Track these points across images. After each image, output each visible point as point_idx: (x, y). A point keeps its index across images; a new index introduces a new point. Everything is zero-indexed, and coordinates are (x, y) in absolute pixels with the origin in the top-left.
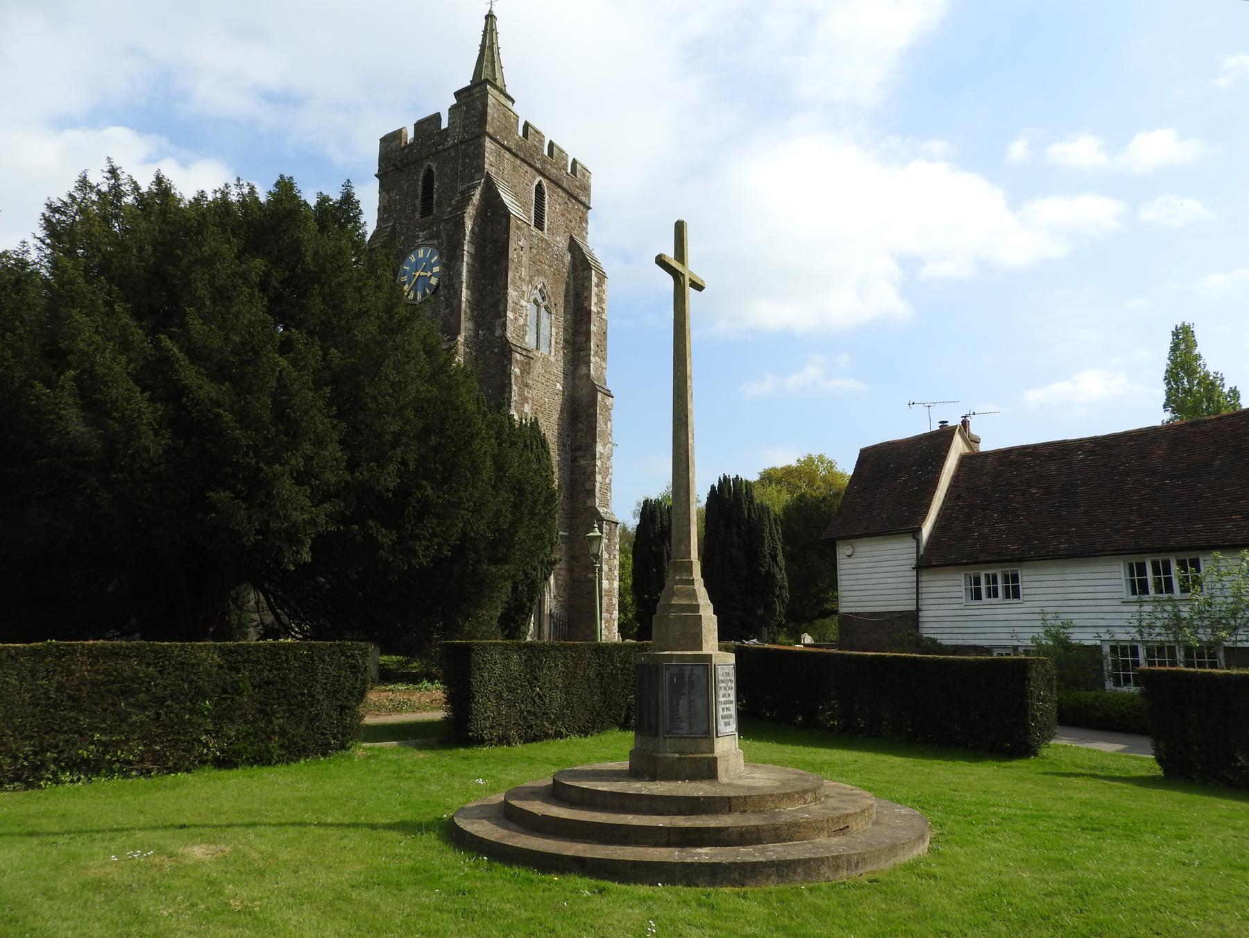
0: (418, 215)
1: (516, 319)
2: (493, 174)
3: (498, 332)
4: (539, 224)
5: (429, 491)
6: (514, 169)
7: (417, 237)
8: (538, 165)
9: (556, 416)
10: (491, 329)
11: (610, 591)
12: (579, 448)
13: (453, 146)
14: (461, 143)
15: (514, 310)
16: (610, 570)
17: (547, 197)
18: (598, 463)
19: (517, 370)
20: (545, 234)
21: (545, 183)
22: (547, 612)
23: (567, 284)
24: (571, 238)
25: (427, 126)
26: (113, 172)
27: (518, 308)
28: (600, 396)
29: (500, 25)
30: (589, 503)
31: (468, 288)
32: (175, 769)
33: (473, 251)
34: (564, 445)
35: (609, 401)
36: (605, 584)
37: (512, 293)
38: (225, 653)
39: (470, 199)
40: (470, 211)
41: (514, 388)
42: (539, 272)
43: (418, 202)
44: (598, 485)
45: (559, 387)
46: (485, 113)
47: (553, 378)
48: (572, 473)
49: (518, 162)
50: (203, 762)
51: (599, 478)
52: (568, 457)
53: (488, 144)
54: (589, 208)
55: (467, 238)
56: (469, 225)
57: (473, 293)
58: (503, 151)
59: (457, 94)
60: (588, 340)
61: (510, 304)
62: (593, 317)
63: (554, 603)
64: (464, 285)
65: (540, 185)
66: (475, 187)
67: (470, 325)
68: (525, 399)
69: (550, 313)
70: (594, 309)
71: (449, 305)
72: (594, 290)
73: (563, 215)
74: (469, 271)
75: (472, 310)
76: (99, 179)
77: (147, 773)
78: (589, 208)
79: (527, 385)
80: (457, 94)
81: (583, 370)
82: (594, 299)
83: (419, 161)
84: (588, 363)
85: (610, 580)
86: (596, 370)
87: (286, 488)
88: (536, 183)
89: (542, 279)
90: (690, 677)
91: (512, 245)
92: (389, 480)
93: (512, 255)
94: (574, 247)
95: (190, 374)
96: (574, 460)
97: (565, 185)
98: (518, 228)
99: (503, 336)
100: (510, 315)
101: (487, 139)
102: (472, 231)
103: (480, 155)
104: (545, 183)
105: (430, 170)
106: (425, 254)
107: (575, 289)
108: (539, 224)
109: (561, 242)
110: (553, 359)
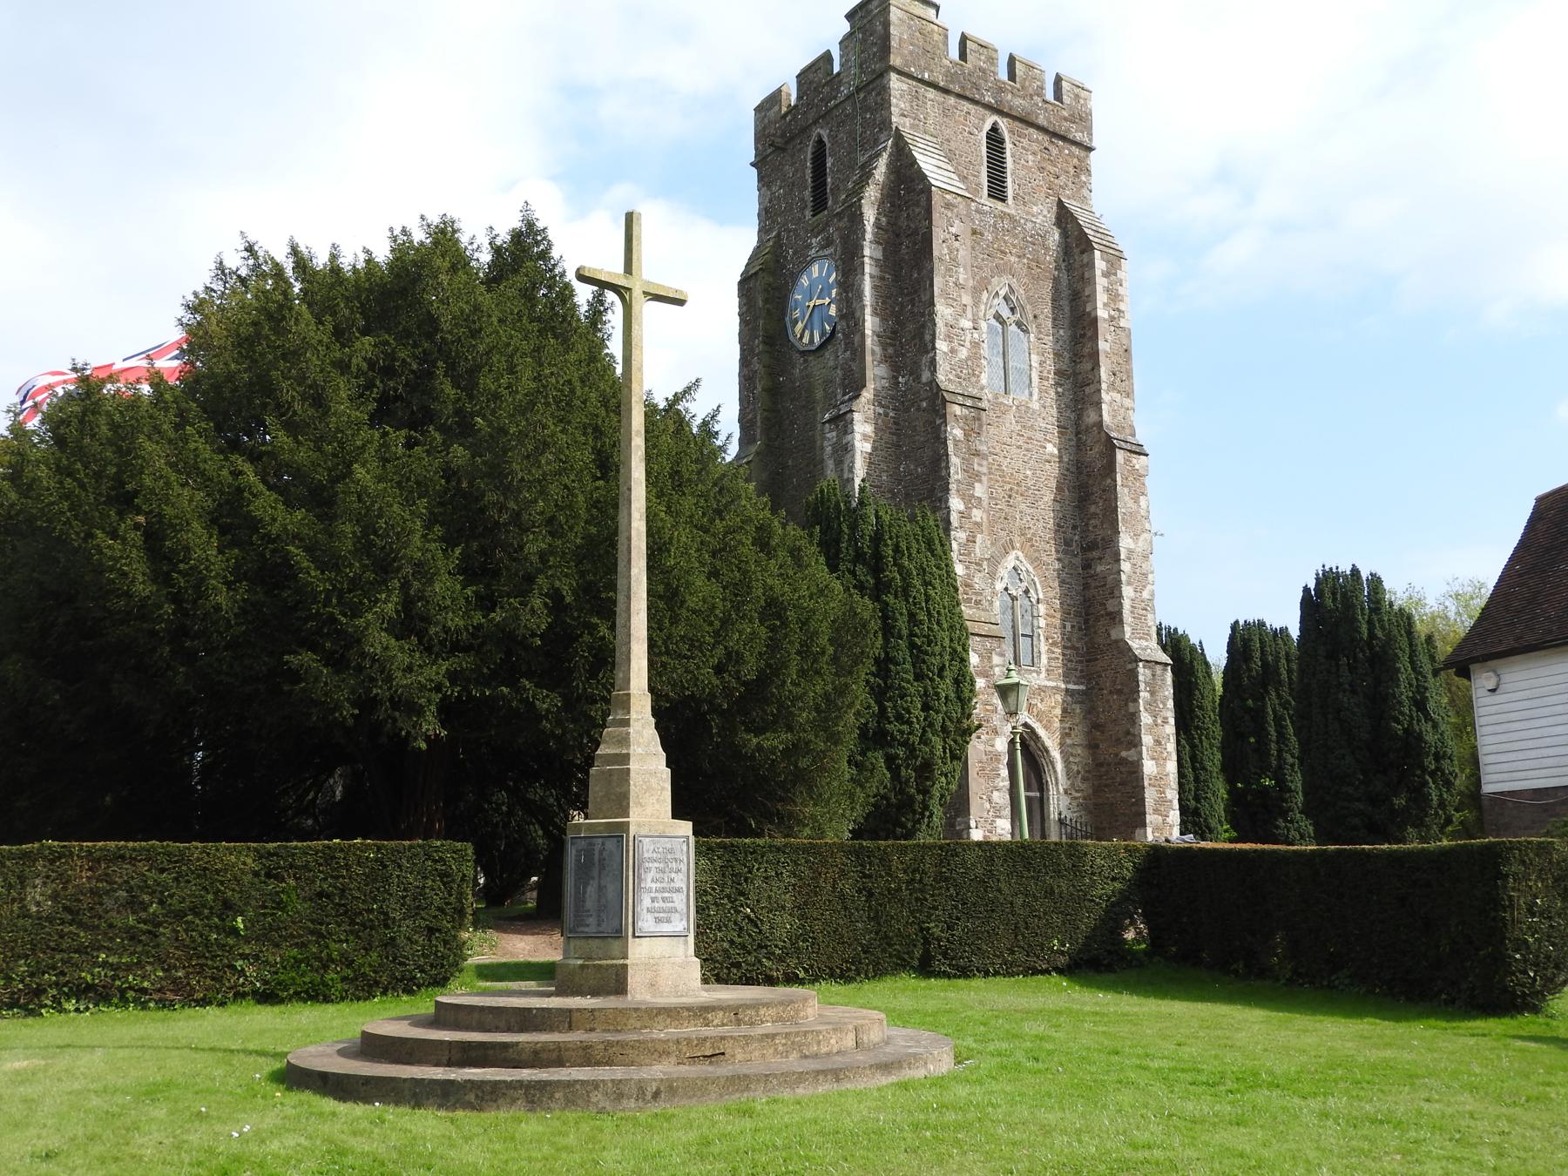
0: (808, 213)
1: (953, 351)
2: (906, 131)
3: (925, 376)
4: (997, 190)
6: (946, 112)
7: (809, 247)
8: (989, 99)
9: (1049, 497)
10: (915, 374)
11: (1159, 779)
12: (1092, 546)
13: (848, 98)
14: (858, 90)
15: (949, 338)
16: (1158, 742)
17: (1008, 146)
18: (1125, 566)
20: (1010, 207)
21: (1004, 124)
22: (1054, 816)
23: (1056, 280)
24: (1060, 204)
25: (815, 76)
26: (250, 249)
27: (953, 333)
28: (1120, 456)
30: (1114, 635)
31: (875, 313)
32: (204, 1002)
33: (879, 255)
34: (1067, 543)
35: (1139, 462)
36: (1149, 767)
37: (943, 311)
38: (260, 856)
39: (870, 175)
40: (872, 194)
41: (955, 460)
42: (999, 270)
43: (807, 194)
44: (1127, 604)
45: (1052, 449)
46: (887, 36)
47: (1039, 436)
48: (1086, 587)
49: (952, 100)
50: (240, 996)
51: (1127, 592)
52: (1078, 561)
53: (896, 83)
54: (1090, 149)
55: (869, 236)
56: (870, 215)
57: (884, 320)
58: (922, 89)
59: (849, 16)
60: (1096, 366)
61: (941, 328)
62: (1102, 326)
63: (1065, 801)
64: (868, 311)
65: (994, 129)
66: (878, 155)
67: (882, 371)
68: (976, 477)
69: (1026, 331)
70: (1102, 313)
71: (849, 345)
72: (1101, 282)
73: (1042, 169)
74: (875, 287)
75: (884, 346)
76: (236, 261)
77: (165, 1004)
78: (1090, 149)
79: (977, 454)
80: (849, 16)
81: (1091, 417)
82: (1101, 298)
83: (805, 130)
84: (1098, 404)
85: (1159, 759)
87: (378, 641)
88: (987, 127)
89: (1006, 279)
90: (601, 853)
91: (938, 235)
92: (534, 616)
93: (939, 249)
94: (1064, 218)
95: (265, 505)
96: (1087, 566)
97: (1041, 121)
98: (948, 206)
99: (933, 382)
100: (941, 346)
101: (893, 76)
102: (877, 225)
103: (885, 104)
104: (1004, 124)
105: (820, 142)
106: (820, 272)
107: (1070, 285)
108: (997, 190)
109: (1042, 215)
110: (1035, 406)
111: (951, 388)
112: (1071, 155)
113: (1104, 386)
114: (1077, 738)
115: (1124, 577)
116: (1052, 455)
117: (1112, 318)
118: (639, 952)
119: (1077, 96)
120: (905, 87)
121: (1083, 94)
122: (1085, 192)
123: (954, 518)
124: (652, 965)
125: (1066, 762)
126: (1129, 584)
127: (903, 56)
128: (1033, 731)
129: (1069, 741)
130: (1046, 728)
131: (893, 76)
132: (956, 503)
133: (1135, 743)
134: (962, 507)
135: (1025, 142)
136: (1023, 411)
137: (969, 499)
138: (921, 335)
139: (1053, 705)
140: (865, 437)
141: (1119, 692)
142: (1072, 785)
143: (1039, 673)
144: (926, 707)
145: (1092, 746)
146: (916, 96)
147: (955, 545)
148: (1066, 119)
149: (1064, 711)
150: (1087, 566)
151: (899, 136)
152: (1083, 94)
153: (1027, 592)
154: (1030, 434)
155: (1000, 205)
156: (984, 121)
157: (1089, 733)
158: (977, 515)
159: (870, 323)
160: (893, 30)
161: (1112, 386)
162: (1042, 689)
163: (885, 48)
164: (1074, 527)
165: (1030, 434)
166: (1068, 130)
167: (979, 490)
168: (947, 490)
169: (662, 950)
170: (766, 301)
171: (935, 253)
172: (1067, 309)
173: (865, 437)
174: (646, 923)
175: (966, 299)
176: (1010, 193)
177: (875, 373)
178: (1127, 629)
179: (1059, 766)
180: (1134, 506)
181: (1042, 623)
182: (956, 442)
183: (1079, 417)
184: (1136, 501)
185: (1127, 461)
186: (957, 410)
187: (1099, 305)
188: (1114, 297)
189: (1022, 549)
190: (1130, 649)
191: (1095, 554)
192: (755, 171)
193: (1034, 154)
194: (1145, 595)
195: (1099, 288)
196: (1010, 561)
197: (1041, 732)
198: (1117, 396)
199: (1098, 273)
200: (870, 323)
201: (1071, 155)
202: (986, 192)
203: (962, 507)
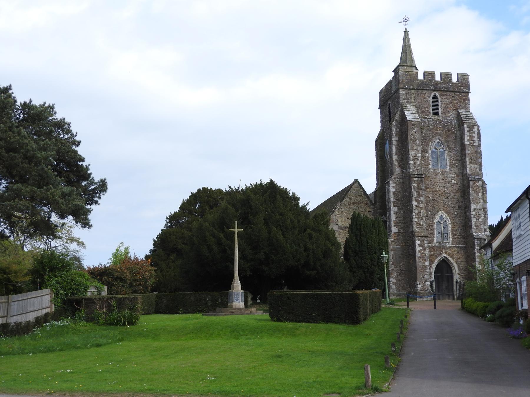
1: (415, 163)
4: (436, 113)
5: (274, 257)
6: (418, 95)
8: (433, 88)
10: (406, 170)
15: (414, 160)
17: (439, 99)
18: (473, 213)
19: (415, 185)
22: (455, 281)
26: (230, 187)
28: (471, 183)
29: (410, 35)
33: (397, 139)
35: (479, 184)
37: (412, 153)
41: (414, 192)
42: (435, 135)
44: (473, 223)
48: (465, 218)
49: (420, 91)
51: (474, 220)
52: (463, 211)
53: (401, 92)
57: (399, 156)
60: (465, 158)
61: (411, 156)
63: (458, 276)
65: (435, 95)
68: (420, 195)
70: (467, 142)
72: (467, 134)
74: (396, 148)
75: (399, 163)
79: (421, 189)
81: (465, 172)
82: (467, 138)
83: (387, 101)
84: (466, 168)
86: (471, 170)
92: (262, 256)
93: (411, 136)
94: (459, 115)
96: (465, 213)
97: (451, 89)
98: (413, 125)
100: (411, 162)
101: (401, 90)
102: (396, 131)
104: (437, 94)
108: (436, 113)
109: (451, 116)
110: (448, 171)
111: (414, 173)
112: (462, 96)
113: (468, 163)
114: (463, 259)
115: (472, 216)
116: (454, 183)
117: (471, 143)
118: (234, 304)
119: (464, 79)
120: (404, 92)
121: (466, 77)
122: (467, 106)
123: (414, 207)
124: (236, 305)
125: (459, 266)
126: (474, 217)
127: (403, 84)
128: (447, 258)
129: (459, 260)
130: (451, 257)
131: (401, 90)
132: (415, 203)
133: (475, 261)
134: (416, 204)
135: (445, 97)
136: (444, 174)
137: (418, 201)
138: (406, 159)
139: (454, 251)
140: (394, 187)
141: (472, 247)
142: (461, 272)
143: (449, 243)
144: (371, 261)
145: (467, 262)
146: (407, 94)
147: (414, 214)
148: (460, 86)
149: (458, 252)
150: (465, 213)
151: (402, 107)
152: (466, 77)
153: (445, 221)
154: (446, 178)
155: (436, 117)
156: (431, 94)
157: (466, 258)
158: (421, 205)
159: (395, 157)
160: (400, 78)
161: (471, 163)
162: (449, 247)
163: (399, 83)
164: (462, 202)
165: (446, 178)
166: (461, 89)
167: (422, 199)
168: (412, 200)
169: (238, 303)
170: (380, 147)
171: (409, 138)
172: (459, 141)
173: (394, 187)
174: (235, 301)
175: (419, 148)
176: (440, 112)
177: (397, 170)
178: (474, 230)
179: (456, 267)
180: (476, 196)
181: (450, 229)
182: (414, 187)
183: (463, 172)
184: (477, 194)
185: (474, 184)
186: (415, 179)
187: (466, 140)
188: (471, 137)
189: (443, 210)
190: (473, 235)
191: (467, 209)
192: (379, 110)
193: (449, 99)
194: (480, 220)
195: (466, 136)
196: (440, 214)
197: (450, 258)
198: (473, 165)
199: (466, 131)
200: (395, 157)
201: (462, 96)
202: (432, 114)
203: (416, 204)
